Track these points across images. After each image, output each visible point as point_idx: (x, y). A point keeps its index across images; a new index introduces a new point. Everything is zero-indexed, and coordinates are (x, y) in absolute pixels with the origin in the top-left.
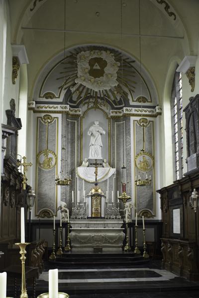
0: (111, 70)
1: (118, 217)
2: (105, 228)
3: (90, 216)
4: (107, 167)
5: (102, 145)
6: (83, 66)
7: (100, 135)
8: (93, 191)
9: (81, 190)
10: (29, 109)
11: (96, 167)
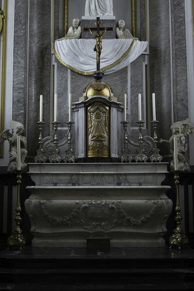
1: (153, 158)
2: (119, 184)
3: (82, 155)
4: (126, 37)
8: (90, 93)
9: (62, 95)
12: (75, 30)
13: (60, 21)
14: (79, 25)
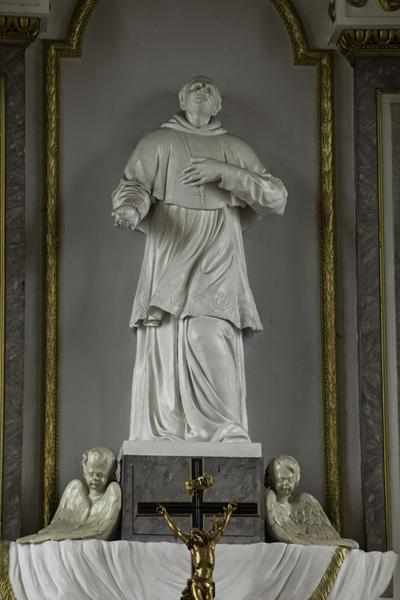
4: (307, 533)
5: (256, 323)
7: (233, 224)
11: (201, 543)
12: (93, 495)
13: (28, 449)
14: (111, 479)
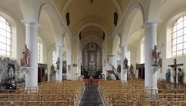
0: (95, 46)
6: (90, 46)
10: (82, 54)
